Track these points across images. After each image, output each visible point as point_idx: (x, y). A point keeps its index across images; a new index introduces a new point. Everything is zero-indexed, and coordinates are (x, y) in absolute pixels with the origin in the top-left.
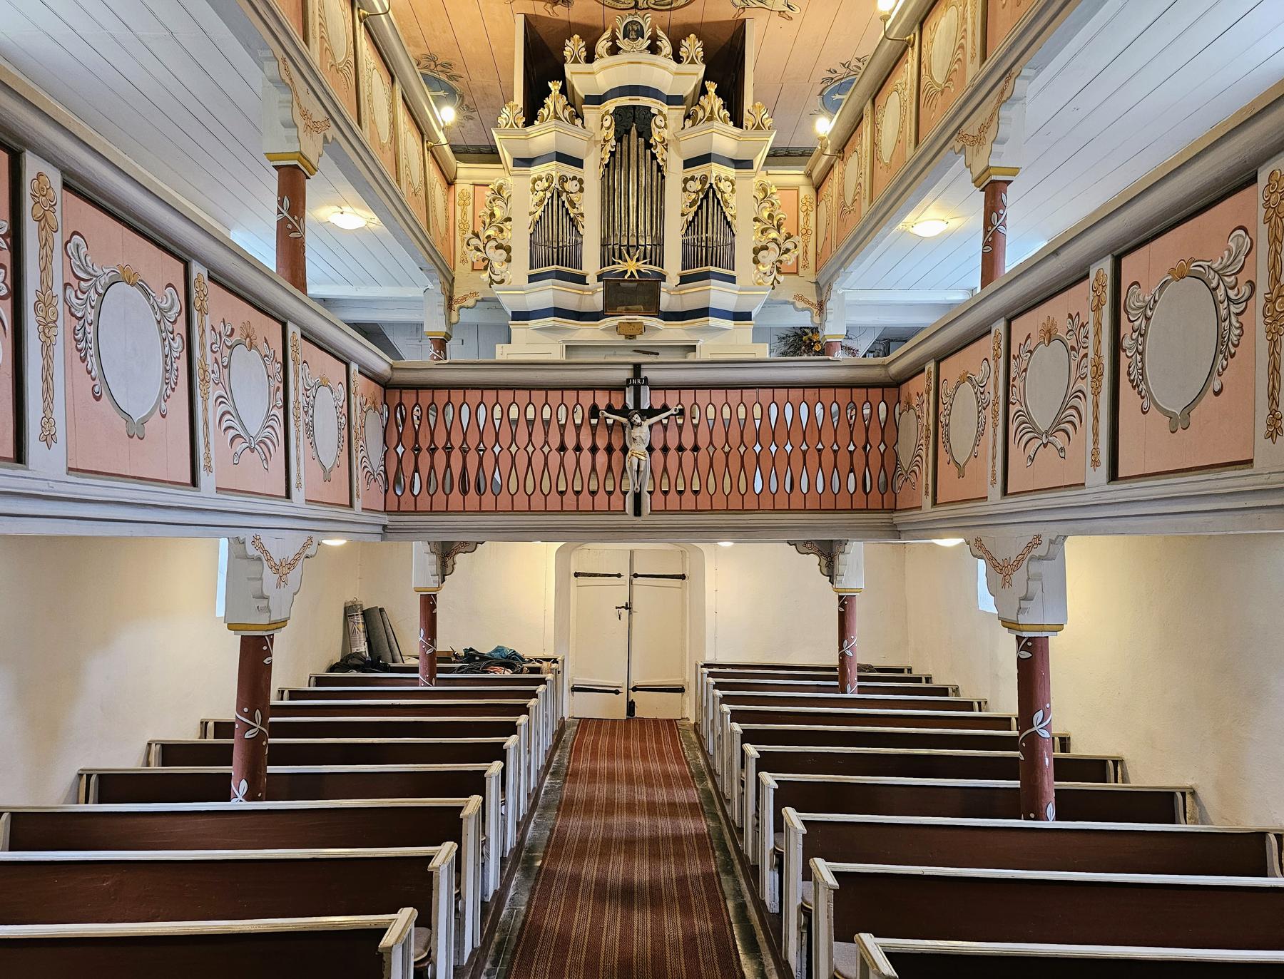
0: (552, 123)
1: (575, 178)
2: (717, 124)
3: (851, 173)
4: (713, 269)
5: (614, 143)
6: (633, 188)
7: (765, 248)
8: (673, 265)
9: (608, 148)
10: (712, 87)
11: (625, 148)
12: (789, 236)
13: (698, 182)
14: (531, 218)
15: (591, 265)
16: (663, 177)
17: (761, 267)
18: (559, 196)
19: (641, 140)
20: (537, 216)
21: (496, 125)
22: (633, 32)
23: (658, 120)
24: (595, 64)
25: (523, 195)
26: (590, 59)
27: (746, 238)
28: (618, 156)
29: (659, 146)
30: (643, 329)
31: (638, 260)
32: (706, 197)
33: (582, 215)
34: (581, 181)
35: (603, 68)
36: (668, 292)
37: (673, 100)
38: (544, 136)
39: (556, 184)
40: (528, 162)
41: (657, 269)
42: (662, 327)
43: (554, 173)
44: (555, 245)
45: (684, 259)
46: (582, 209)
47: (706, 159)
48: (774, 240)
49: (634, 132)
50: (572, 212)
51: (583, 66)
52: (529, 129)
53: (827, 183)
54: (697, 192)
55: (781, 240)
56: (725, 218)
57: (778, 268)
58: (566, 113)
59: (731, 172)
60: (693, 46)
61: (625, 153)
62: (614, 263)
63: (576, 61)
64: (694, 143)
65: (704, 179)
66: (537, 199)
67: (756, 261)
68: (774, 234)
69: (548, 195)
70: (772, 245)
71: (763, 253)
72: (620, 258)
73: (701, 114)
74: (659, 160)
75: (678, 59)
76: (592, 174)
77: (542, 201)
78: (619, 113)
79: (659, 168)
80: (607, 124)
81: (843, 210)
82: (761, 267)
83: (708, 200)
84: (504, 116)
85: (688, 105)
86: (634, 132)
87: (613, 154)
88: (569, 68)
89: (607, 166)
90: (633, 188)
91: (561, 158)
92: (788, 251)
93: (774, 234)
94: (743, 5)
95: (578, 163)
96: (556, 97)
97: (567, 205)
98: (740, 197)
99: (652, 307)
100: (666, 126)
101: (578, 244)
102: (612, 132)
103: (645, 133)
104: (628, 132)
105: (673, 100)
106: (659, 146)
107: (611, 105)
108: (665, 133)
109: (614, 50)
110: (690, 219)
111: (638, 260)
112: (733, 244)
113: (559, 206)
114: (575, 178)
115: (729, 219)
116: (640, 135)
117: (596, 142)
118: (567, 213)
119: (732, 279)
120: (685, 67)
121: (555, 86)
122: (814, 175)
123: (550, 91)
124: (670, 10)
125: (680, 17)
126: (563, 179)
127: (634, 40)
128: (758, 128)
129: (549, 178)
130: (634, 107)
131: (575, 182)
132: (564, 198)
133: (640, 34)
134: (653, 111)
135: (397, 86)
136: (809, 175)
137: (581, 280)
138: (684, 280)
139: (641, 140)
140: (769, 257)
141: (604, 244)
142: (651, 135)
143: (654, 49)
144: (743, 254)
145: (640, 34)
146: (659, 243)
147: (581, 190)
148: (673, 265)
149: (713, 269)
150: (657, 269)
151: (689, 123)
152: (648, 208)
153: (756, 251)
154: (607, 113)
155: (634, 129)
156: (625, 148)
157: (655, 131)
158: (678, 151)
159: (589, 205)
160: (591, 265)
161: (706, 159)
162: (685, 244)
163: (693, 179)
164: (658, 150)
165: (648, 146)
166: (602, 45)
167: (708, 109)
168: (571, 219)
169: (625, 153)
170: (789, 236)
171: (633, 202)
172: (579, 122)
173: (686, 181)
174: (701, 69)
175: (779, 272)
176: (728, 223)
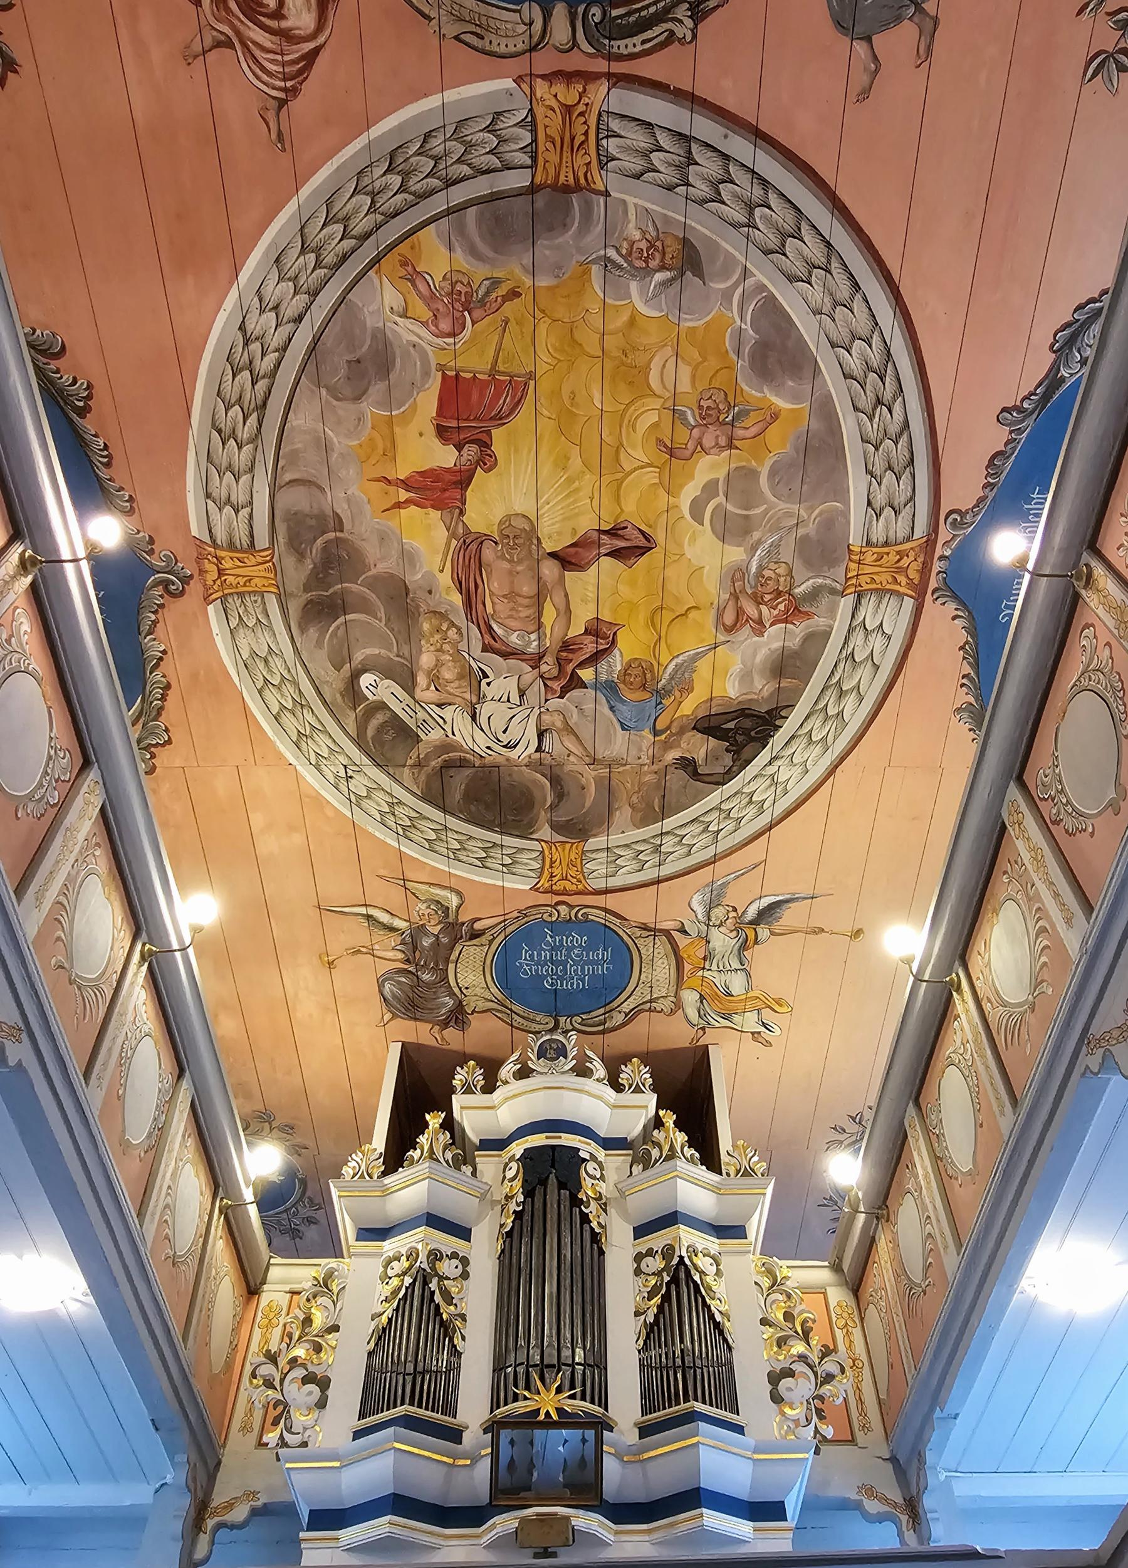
0: (424, 1166)
1: (454, 1255)
2: (681, 1164)
3: (913, 1223)
4: (699, 1407)
5: (521, 1198)
6: (551, 1264)
7: (790, 1373)
8: (625, 1401)
9: (513, 1207)
10: (669, 1118)
11: (538, 1204)
12: (826, 1352)
13: (658, 1258)
14: (373, 1324)
15: (473, 1404)
16: (602, 1253)
17: (788, 1411)
18: (425, 1283)
19: (565, 1193)
20: (384, 1319)
21: (339, 1175)
22: (552, 1052)
23: (591, 1167)
24: (498, 1095)
25: (367, 1283)
26: (489, 1088)
27: (752, 1357)
28: (527, 1217)
29: (593, 1204)
30: (572, 1537)
31: (559, 1390)
32: (675, 1280)
33: (463, 1317)
34: (465, 1261)
35: (507, 1099)
36: (618, 1456)
37: (609, 1144)
38: (411, 1190)
39: (422, 1261)
40: (380, 1233)
41: (596, 1409)
42: (609, 1537)
43: (420, 1246)
44: (410, 1368)
45: (643, 1396)
46: (463, 1307)
47: (671, 1219)
48: (802, 1358)
49: (552, 1180)
50: (447, 1311)
51: (479, 1099)
52: (388, 1180)
53: (873, 1269)
54: (659, 1274)
55: (814, 1358)
56: (712, 1316)
57: (819, 1412)
58: (449, 1155)
59: (712, 1244)
60: (635, 1072)
61: (538, 1214)
62: (516, 1398)
63: (468, 1090)
64: (647, 1198)
65: (668, 1252)
66: (387, 1290)
67: (777, 1398)
68: (799, 1348)
69: (408, 1280)
70: (800, 1367)
71: (786, 1383)
72: (527, 1388)
73: (655, 1153)
74: (594, 1224)
75: (618, 1088)
76: (484, 1251)
77: (395, 1292)
78: (529, 1156)
79: (595, 1238)
80: (510, 1174)
81: (910, 1293)
82: (788, 1411)
83: (679, 1288)
84: (352, 1164)
85: (638, 1150)
86: (552, 1180)
87: (518, 1215)
88: (457, 1101)
89: (509, 1234)
90: (551, 1264)
91: (434, 1221)
92: (829, 1378)
93: (799, 1348)
94: (702, 1023)
95: (464, 1233)
96: (436, 1132)
97: (438, 1298)
98: (734, 1283)
99: (584, 1488)
100: (602, 1178)
101: (453, 1369)
102: (518, 1184)
103: (571, 1183)
104: (544, 1182)
105: (609, 1144)
106: (593, 1204)
107: (517, 1149)
108: (602, 1187)
109: (524, 1073)
110: (651, 1319)
111: (559, 1390)
112: (730, 1363)
113: (423, 1305)
114: (454, 1255)
115: (718, 1318)
116: (562, 1186)
117: (493, 1203)
118: (438, 1312)
119: (739, 1429)
120: (628, 1097)
121: (434, 1120)
122: (846, 1269)
123: (426, 1125)
124: (603, 1032)
125: (617, 1042)
126: (435, 1256)
127: (552, 1059)
128: (746, 1174)
129: (412, 1255)
130: (553, 1147)
131: (455, 1262)
132: (433, 1285)
133: (562, 1052)
134: (582, 1154)
135: (186, 1084)
136: (837, 1268)
137: (454, 1435)
138: (645, 1431)
139: (565, 1193)
140: (800, 1388)
141: (499, 1367)
142: (579, 1187)
143: (582, 1071)
144: (751, 1384)
145: (562, 1052)
146: (598, 1363)
147: (465, 1275)
148: (625, 1401)
149: (699, 1407)
150: (596, 1409)
151: (637, 1169)
152: (578, 1298)
153: (775, 1378)
154: (512, 1159)
155: (552, 1176)
156: (538, 1204)
157: (587, 1183)
158: (625, 1215)
159: (477, 1303)
160: (473, 1404)
161: (671, 1219)
162: (644, 1366)
163: (650, 1253)
164: (593, 1209)
165: (576, 1202)
166: (507, 1071)
167: (666, 1148)
168: (442, 1323)
169: (538, 1214)
170: (826, 1352)
171: (550, 1288)
172: (467, 1169)
173: (639, 1258)
174: (651, 1099)
175: (821, 1417)
176: (717, 1325)
